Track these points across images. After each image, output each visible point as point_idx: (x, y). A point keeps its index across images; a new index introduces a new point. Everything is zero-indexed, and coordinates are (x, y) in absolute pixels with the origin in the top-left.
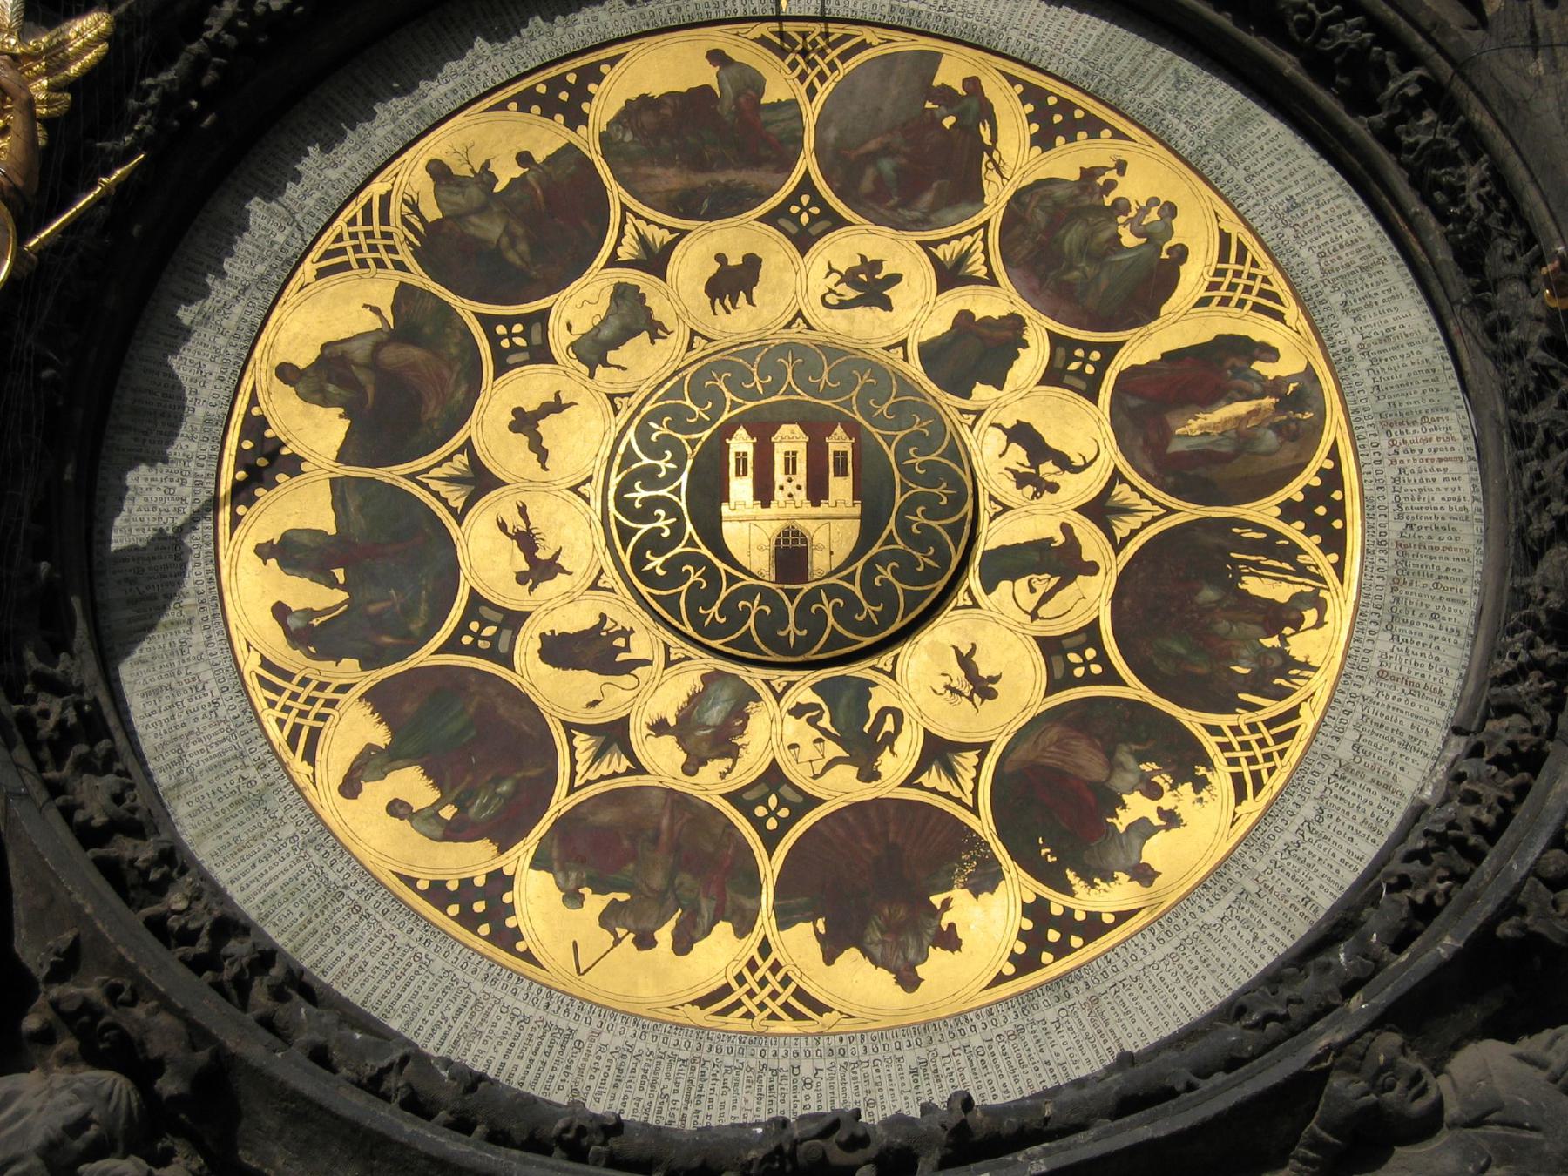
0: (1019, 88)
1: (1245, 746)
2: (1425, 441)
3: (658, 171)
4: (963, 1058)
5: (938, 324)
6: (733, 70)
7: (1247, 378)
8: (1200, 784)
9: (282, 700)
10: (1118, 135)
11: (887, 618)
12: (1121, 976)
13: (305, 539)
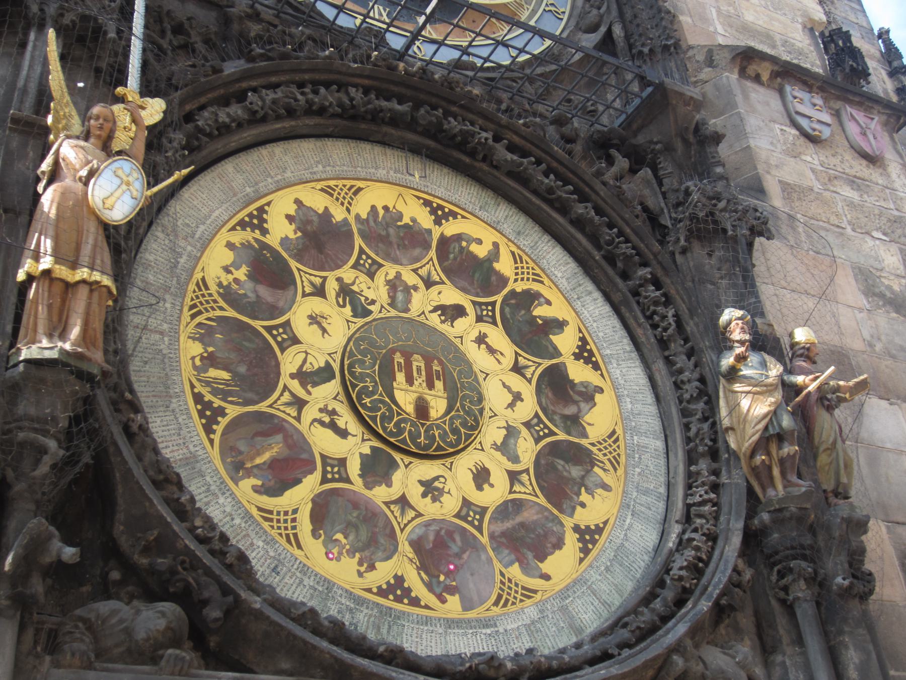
2: (173, 451)
3: (535, 517)
5: (397, 477)
6: (537, 574)
8: (220, 285)
10: (369, 590)
13: (556, 331)
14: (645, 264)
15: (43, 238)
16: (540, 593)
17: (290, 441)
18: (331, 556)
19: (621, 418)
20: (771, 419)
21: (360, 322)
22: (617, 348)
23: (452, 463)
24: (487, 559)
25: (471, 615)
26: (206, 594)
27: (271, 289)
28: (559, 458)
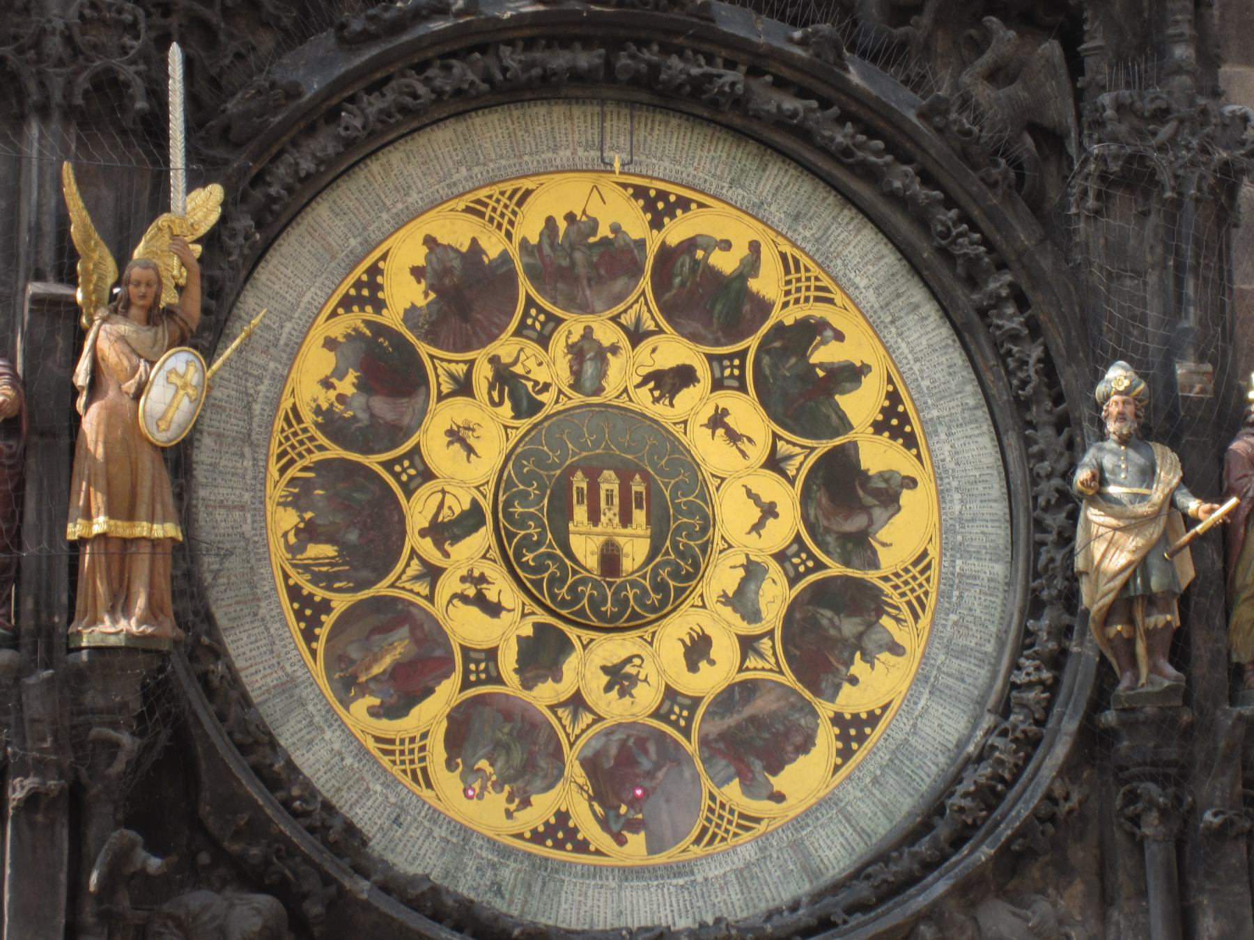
2: (265, 676)
3: (774, 707)
4: (388, 203)
5: (570, 665)
6: (765, 793)
8: (318, 411)
9: (813, 283)
10: (520, 836)
11: (509, 516)
12: (324, 276)
13: (848, 385)
14: (1001, 266)
15: (92, 489)
16: (764, 823)
17: (419, 634)
18: (470, 793)
19: (940, 530)
20: (1135, 571)
21: (525, 424)
22: (952, 404)
23: (654, 633)
24: (692, 776)
25: (659, 859)
26: (306, 888)
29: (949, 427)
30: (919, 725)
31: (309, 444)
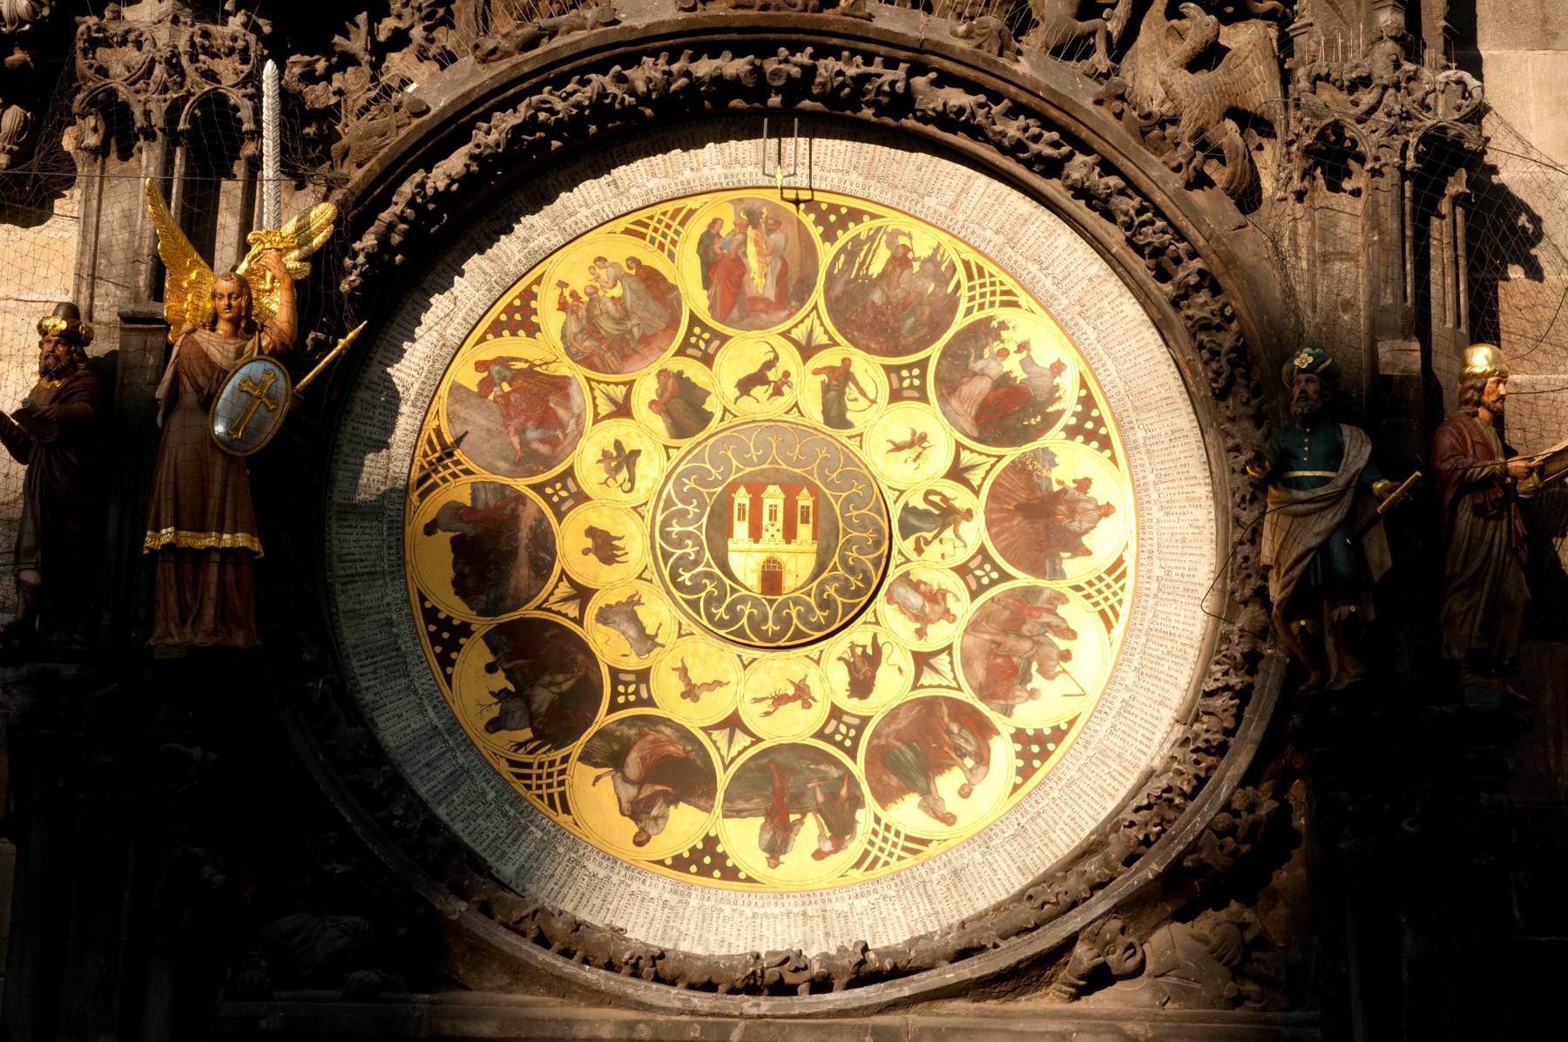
0: (490, 336)
1: (983, 295)
3: (513, 582)
4: (1162, 487)
5: (659, 424)
6: (442, 520)
7: (731, 242)
8: (1003, 325)
9: (884, 857)
10: (538, 281)
13: (767, 837)
21: (895, 512)
22: (692, 927)
27: (980, 398)
28: (573, 687)
29: (672, 908)
30: (413, 697)
31: (978, 301)
